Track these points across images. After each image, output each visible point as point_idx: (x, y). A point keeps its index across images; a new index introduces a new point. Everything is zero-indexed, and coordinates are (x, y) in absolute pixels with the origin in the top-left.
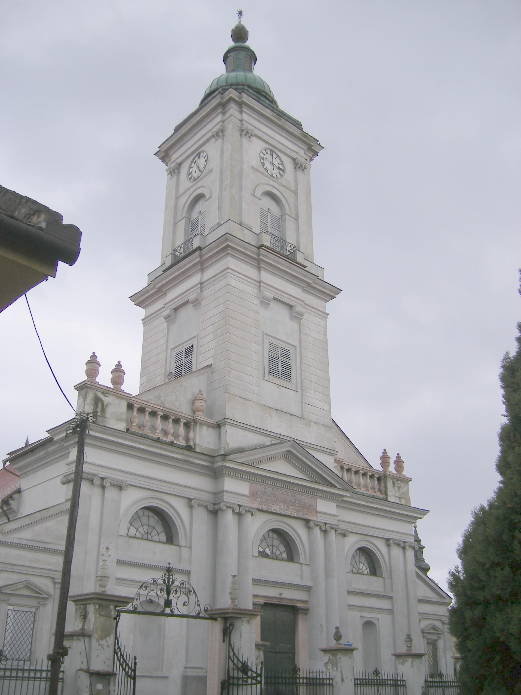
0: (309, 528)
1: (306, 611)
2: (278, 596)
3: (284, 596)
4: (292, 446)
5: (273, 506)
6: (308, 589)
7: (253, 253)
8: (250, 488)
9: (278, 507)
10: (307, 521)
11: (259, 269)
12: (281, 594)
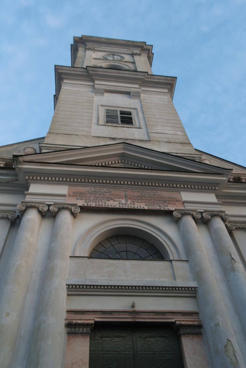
0: (177, 221)
1: (197, 330)
2: (130, 309)
3: (138, 308)
4: (124, 149)
5: (107, 202)
6: (191, 293)
7: (83, 72)
8: (68, 189)
9: (117, 203)
10: (168, 214)
11: (93, 81)
12: (133, 306)
